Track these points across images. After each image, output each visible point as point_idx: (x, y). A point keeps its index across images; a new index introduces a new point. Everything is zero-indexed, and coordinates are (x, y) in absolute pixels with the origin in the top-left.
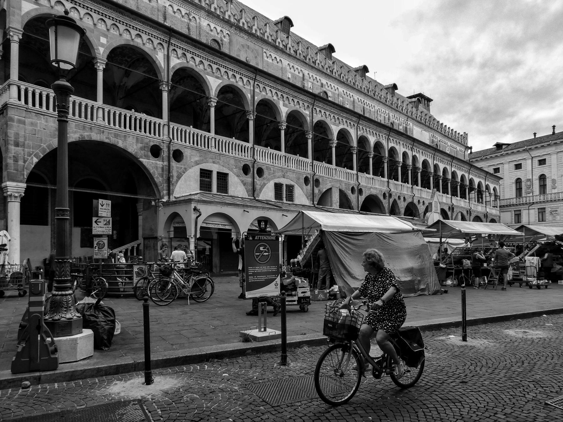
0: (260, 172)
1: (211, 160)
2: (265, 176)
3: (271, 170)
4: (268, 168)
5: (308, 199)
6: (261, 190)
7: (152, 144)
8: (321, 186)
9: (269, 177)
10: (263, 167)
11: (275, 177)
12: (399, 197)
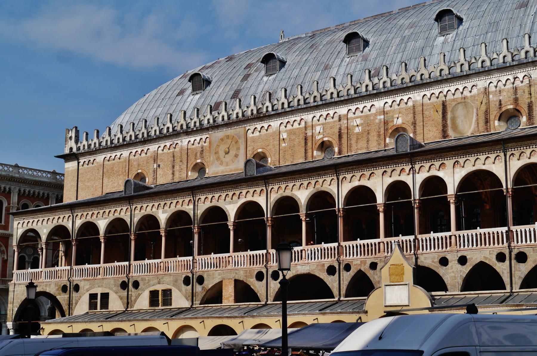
0: (136, 285)
1: (97, 285)
2: (140, 287)
3: (146, 280)
4: (142, 279)
5: (188, 300)
6: (135, 301)
7: (63, 285)
8: (205, 282)
9: (144, 287)
10: (138, 280)
11: (150, 286)
12: (373, 266)
